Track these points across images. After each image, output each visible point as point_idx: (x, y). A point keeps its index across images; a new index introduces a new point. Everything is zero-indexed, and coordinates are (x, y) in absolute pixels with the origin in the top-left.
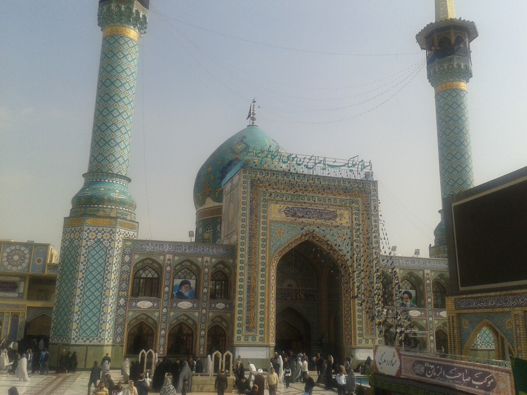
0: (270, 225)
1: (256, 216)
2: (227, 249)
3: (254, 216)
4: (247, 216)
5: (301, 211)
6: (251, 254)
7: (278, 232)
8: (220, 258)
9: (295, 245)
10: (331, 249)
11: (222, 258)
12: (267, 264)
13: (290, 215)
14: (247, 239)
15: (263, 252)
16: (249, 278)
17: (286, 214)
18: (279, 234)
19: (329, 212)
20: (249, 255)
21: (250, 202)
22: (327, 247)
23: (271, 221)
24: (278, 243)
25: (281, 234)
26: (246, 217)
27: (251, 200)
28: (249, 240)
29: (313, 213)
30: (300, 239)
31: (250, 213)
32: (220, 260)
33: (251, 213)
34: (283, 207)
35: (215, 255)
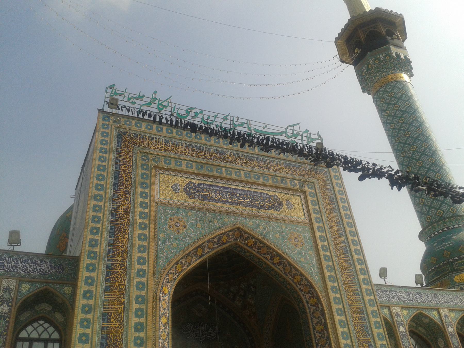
0: (157, 211)
1: (127, 192)
2: (61, 265)
3: (122, 192)
4: (108, 190)
5: (216, 191)
6: (112, 264)
7: (173, 223)
8: (42, 283)
9: (210, 254)
10: (280, 263)
11: (48, 283)
12: (150, 287)
13: (196, 196)
14: (106, 234)
15: (142, 261)
16: (106, 317)
17: (189, 194)
18: (175, 228)
19: (267, 196)
20: (108, 267)
21: (116, 168)
22: (272, 258)
23: (158, 204)
24: (175, 245)
25: (181, 228)
26: (106, 193)
27: (116, 164)
28: (110, 237)
29: (238, 195)
30: (218, 241)
31: (114, 185)
32: (40, 287)
33: (117, 186)
34: (182, 181)
35: (30, 275)
